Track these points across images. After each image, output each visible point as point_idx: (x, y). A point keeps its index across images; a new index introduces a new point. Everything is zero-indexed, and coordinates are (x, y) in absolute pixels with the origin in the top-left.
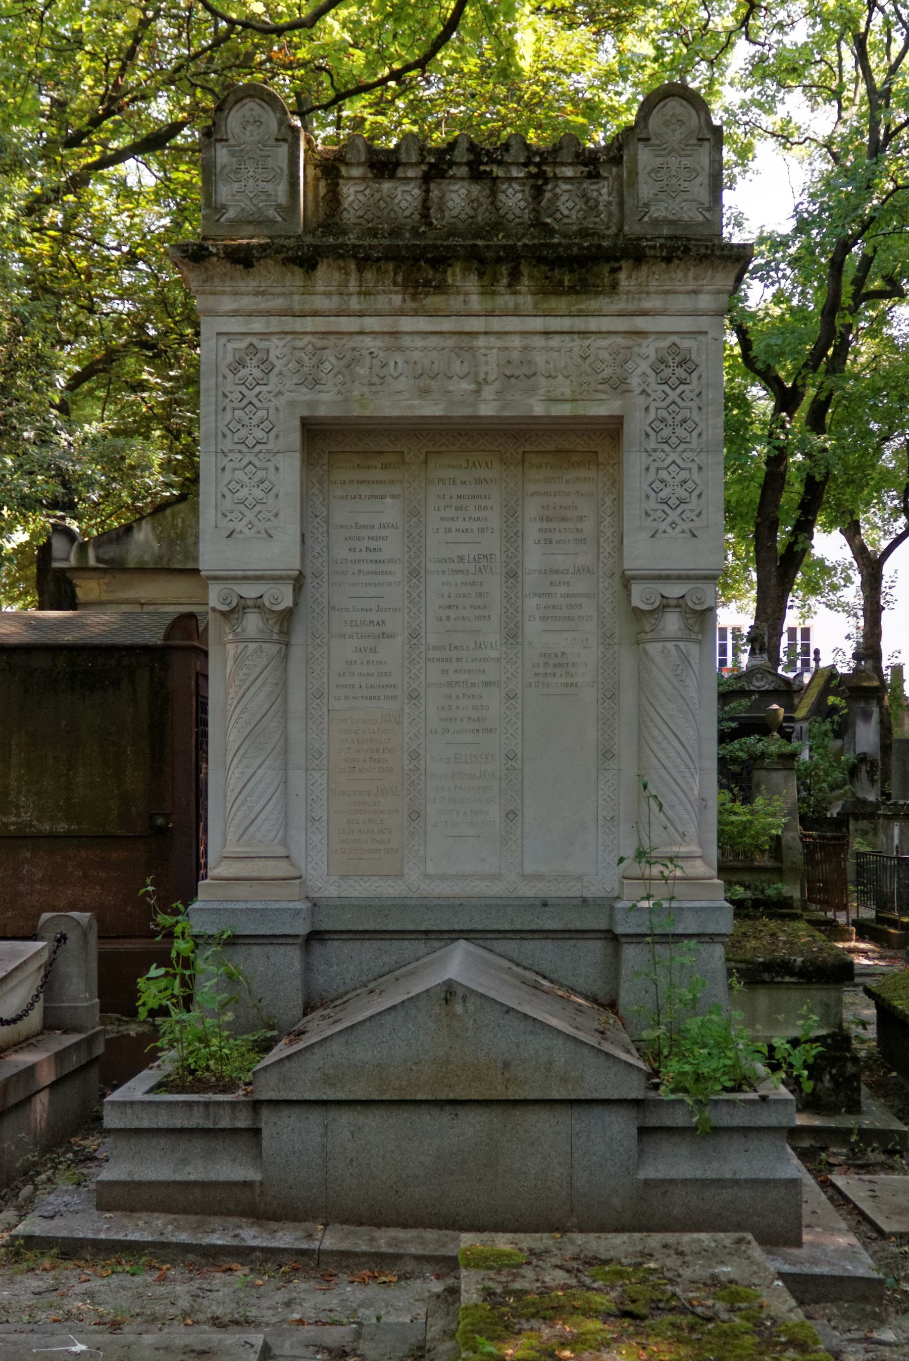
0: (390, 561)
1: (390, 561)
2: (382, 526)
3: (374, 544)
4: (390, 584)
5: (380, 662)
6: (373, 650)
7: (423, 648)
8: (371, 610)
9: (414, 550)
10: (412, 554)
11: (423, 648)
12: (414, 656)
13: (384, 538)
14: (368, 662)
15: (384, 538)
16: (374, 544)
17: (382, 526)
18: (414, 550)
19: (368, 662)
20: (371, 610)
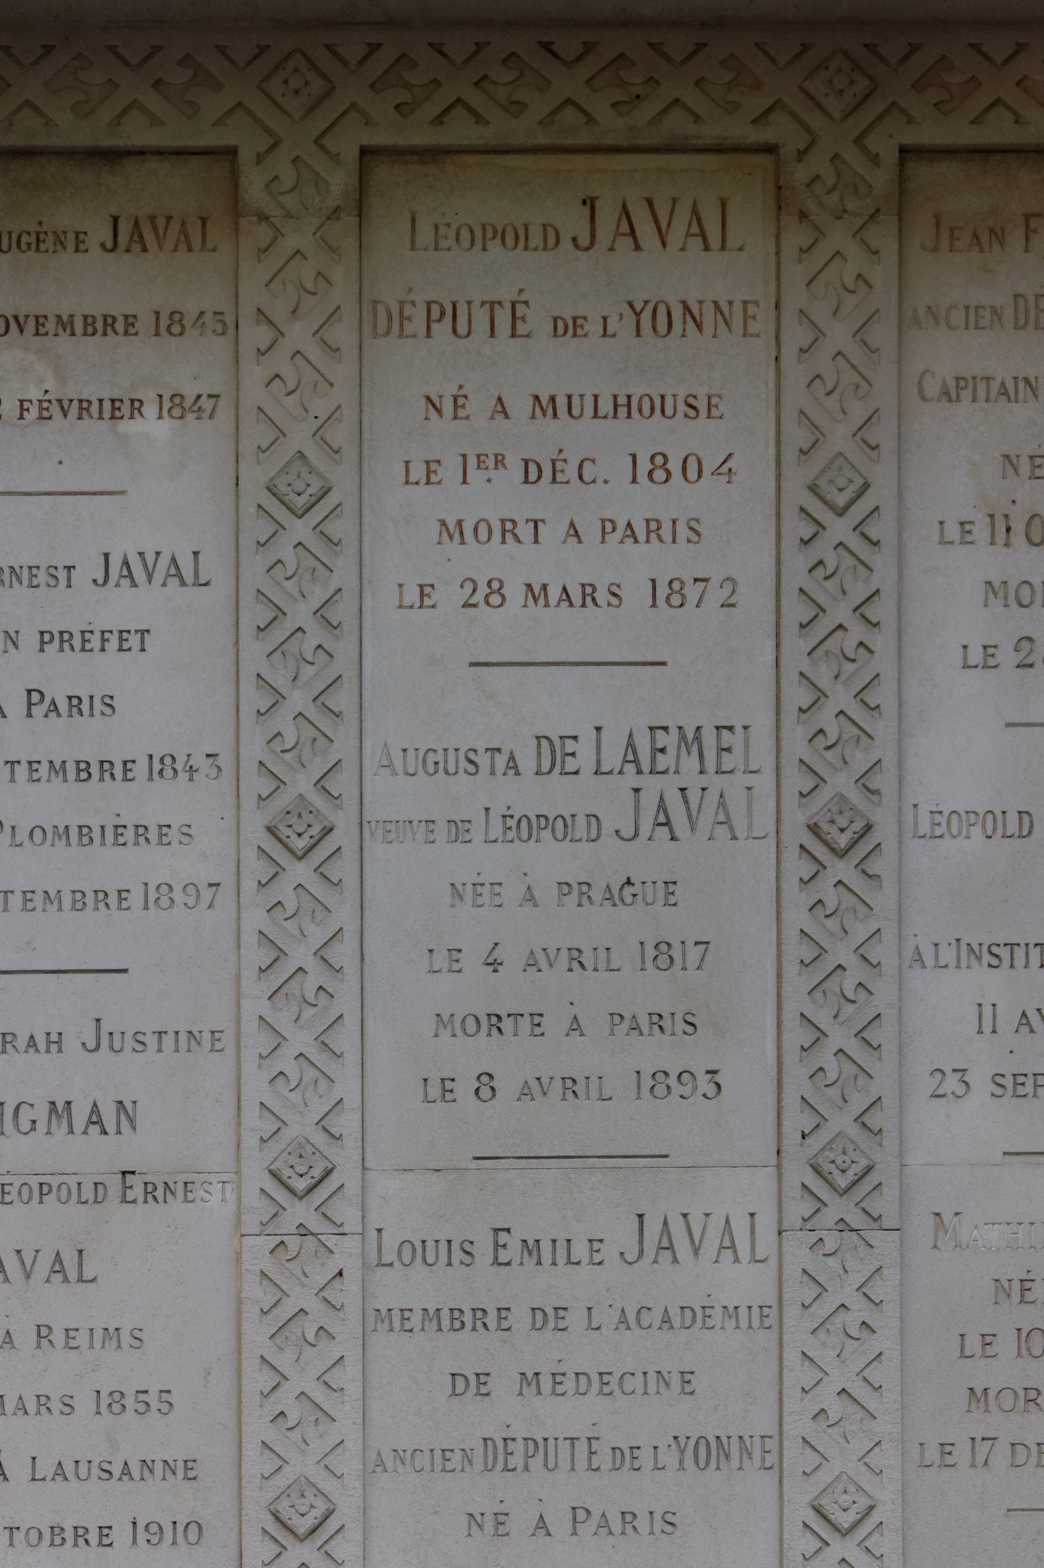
0: (162, 766)
1: (162, 766)
2: (117, 572)
3: (63, 674)
4: (159, 896)
5: (112, 1335)
6: (68, 1269)
7: (347, 1253)
8: (56, 1042)
9: (298, 700)
10: (284, 722)
11: (347, 1253)
12: (301, 1297)
13: (129, 640)
14: (43, 1333)
15: (129, 640)
16: (63, 674)
17: (117, 572)
18: (298, 700)
19: (43, 1333)
20: (56, 1042)
